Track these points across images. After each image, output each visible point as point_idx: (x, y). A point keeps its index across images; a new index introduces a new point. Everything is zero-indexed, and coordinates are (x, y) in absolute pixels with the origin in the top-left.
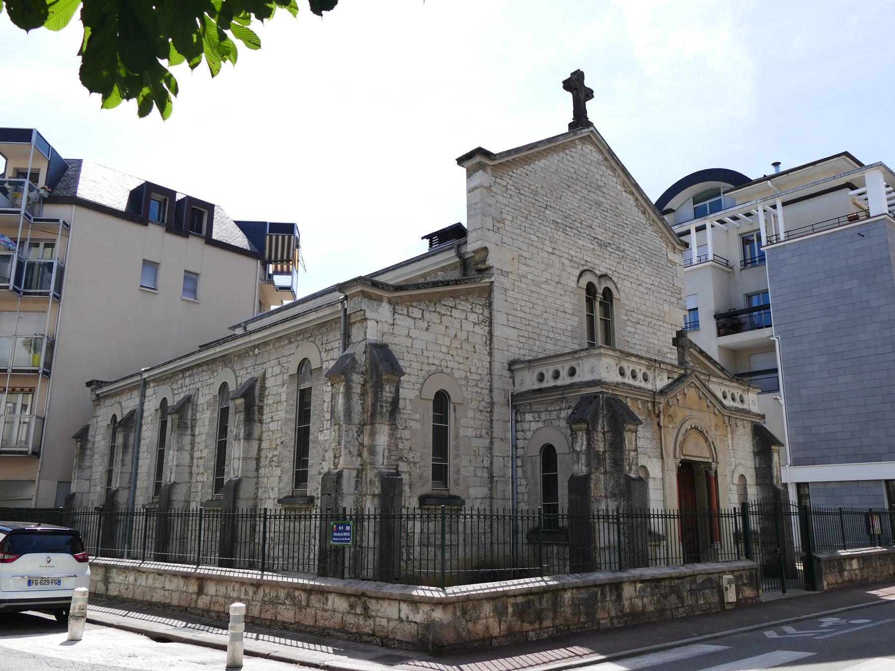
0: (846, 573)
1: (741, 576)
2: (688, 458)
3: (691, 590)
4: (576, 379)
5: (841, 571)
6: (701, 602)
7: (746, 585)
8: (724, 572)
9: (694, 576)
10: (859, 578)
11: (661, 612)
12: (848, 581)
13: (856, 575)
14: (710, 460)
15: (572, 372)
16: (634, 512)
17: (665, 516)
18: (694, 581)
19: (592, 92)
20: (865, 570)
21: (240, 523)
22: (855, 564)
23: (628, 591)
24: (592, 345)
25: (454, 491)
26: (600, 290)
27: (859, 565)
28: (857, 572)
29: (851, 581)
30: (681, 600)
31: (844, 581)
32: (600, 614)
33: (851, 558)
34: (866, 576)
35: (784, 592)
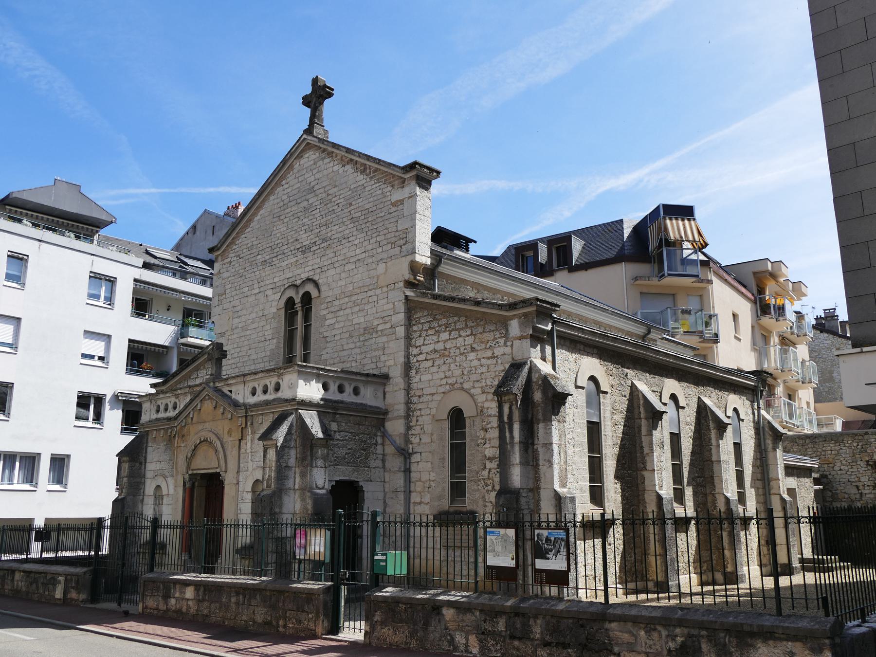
0: (173, 601)
1: (71, 580)
2: (195, 472)
3: (43, 583)
4: (280, 395)
5: (167, 597)
6: (47, 593)
7: (73, 588)
8: (60, 574)
9: (46, 573)
10: (193, 611)
11: (27, 593)
12: (175, 611)
13: (188, 606)
14: (218, 471)
15: (277, 388)
16: (241, 523)
17: (172, 527)
18: (46, 577)
19: (304, 103)
20: (206, 604)
21: (225, 529)
22: (190, 593)
23: (18, 576)
24: (289, 361)
25: (469, 506)
26: (297, 300)
27: (197, 594)
28: (190, 603)
29: (179, 611)
30: (38, 588)
31: (168, 610)
32: (6, 587)
33: (186, 583)
34: (205, 612)
35: (119, 605)
